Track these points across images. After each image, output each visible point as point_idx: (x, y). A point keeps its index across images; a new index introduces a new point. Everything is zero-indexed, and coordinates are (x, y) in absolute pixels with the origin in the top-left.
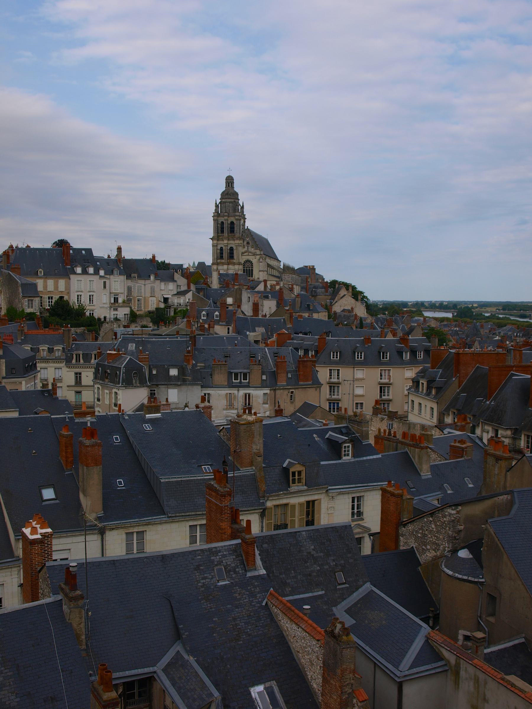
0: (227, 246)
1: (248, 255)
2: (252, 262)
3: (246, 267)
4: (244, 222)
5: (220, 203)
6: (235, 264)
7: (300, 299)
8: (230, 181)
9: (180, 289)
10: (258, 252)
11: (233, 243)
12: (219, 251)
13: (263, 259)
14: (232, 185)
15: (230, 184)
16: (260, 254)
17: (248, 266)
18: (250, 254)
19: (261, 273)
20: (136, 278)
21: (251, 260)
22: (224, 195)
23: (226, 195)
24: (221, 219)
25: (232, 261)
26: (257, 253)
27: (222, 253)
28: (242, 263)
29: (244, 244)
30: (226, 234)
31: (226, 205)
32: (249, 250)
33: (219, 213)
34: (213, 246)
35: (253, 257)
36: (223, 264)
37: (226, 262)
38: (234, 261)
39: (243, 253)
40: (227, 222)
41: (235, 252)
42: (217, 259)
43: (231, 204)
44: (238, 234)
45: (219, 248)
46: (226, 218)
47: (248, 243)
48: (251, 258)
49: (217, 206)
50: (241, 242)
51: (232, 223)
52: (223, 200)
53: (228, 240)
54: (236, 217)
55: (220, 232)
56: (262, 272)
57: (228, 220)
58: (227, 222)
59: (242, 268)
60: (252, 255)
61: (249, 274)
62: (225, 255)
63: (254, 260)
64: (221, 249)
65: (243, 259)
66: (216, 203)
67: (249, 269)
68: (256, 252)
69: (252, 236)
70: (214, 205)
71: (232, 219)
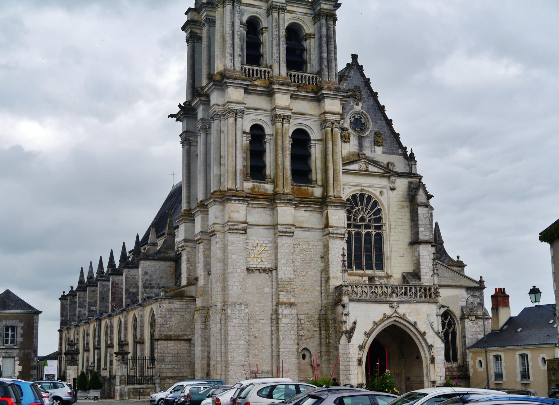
1: (366, 173)
2: (376, 203)
12: (244, 141)
17: (363, 219)
18: (372, 168)
29: (347, 125)
32: (367, 152)
35: (384, 182)
38: (318, 192)
39: (348, 161)
41: (316, 151)
45: (248, 130)
61: (368, 258)
67: (368, 235)
68: (393, 164)
69: (374, 95)
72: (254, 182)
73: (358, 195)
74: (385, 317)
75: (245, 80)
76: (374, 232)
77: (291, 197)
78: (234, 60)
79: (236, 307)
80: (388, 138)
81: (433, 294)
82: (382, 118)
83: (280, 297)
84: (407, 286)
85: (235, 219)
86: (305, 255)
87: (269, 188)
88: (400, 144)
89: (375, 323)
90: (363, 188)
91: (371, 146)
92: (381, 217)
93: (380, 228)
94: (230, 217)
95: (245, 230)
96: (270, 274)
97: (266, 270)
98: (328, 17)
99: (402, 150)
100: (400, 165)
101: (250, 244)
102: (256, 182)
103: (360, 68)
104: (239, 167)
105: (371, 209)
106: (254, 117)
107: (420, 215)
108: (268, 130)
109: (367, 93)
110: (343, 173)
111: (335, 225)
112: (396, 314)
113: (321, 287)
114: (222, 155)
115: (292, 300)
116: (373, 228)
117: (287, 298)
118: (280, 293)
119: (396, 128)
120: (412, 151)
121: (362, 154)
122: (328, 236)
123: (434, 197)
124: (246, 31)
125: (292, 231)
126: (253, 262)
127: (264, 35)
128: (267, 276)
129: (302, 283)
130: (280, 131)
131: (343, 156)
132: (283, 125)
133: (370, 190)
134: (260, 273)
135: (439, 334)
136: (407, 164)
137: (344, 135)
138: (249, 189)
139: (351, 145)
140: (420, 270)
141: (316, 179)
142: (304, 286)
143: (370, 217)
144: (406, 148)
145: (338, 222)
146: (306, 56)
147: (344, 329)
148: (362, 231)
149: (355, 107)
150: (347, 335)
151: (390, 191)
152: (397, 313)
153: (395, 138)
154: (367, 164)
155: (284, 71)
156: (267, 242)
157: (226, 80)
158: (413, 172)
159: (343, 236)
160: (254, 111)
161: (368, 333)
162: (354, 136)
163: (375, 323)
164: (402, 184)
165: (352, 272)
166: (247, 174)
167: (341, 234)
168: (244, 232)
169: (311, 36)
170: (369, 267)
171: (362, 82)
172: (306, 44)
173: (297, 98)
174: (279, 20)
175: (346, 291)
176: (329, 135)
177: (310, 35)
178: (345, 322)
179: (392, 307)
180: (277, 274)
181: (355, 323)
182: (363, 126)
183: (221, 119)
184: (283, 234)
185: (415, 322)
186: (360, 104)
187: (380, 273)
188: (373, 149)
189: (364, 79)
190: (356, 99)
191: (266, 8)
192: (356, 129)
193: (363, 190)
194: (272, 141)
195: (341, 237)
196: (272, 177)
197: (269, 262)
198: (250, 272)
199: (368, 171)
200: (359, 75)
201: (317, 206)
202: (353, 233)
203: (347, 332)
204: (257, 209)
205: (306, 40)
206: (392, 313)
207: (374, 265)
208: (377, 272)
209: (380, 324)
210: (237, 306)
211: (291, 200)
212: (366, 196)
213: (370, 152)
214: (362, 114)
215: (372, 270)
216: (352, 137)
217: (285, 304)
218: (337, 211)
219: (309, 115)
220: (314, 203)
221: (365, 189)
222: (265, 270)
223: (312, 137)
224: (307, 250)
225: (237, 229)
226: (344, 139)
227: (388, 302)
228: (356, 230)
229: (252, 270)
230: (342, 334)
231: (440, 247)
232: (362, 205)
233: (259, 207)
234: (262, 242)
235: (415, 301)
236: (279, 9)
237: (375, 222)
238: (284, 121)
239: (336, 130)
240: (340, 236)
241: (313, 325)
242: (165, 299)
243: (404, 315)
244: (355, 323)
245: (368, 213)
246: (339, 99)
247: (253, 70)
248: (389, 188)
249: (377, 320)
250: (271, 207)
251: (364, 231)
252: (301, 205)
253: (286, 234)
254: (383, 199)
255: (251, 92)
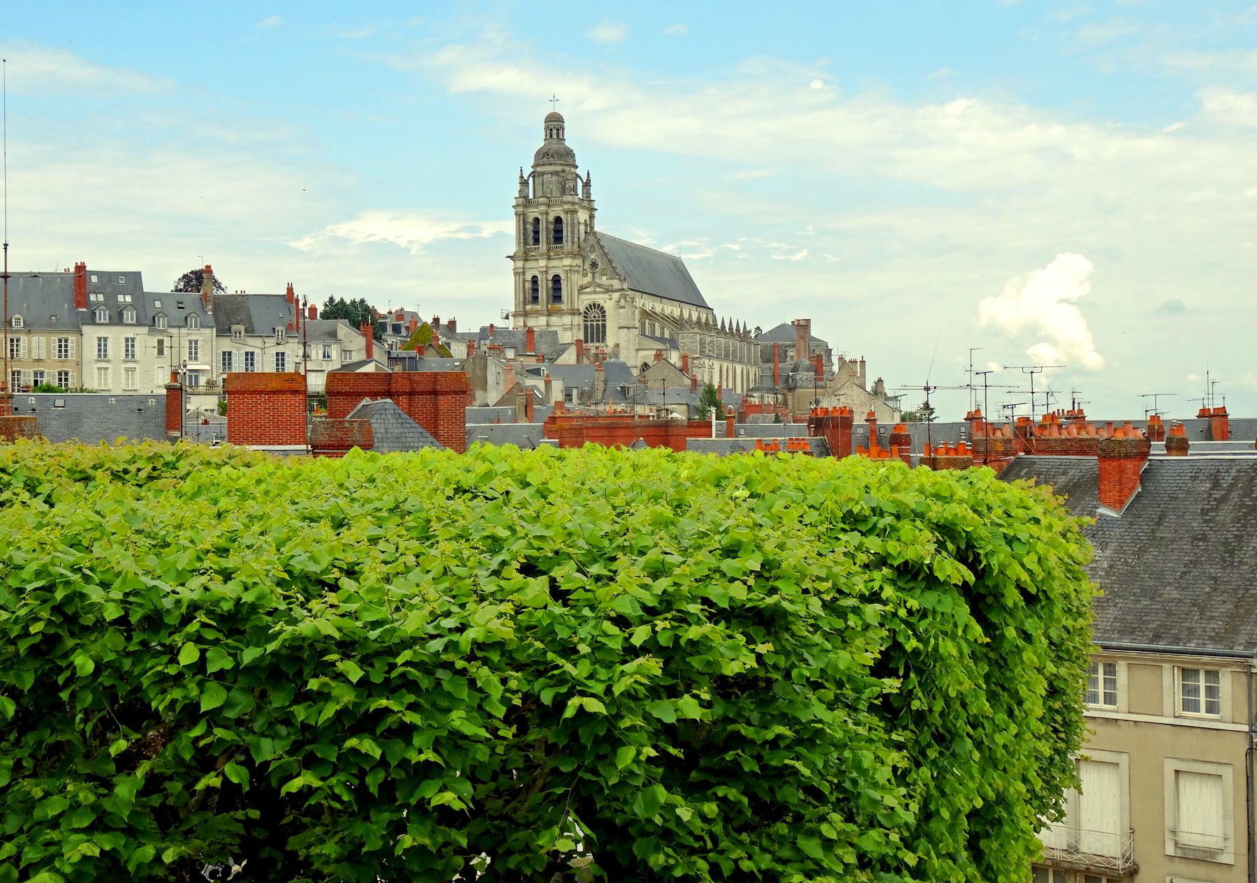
0: (546, 272)
1: (595, 292)
4: (592, 217)
5: (533, 174)
6: (564, 314)
7: (603, 373)
8: (555, 125)
9: (350, 358)
10: (616, 284)
11: (561, 265)
12: (528, 285)
13: (628, 299)
14: (558, 134)
15: (554, 132)
16: (622, 290)
18: (598, 289)
19: (623, 332)
20: (243, 333)
21: (602, 303)
22: (543, 156)
24: (533, 213)
25: (557, 306)
26: (615, 288)
27: (535, 290)
28: (582, 311)
30: (543, 246)
32: (597, 281)
33: (531, 196)
34: (516, 274)
35: (606, 296)
36: (537, 313)
37: (545, 308)
39: (582, 288)
40: (547, 219)
42: (525, 304)
43: (555, 178)
44: (570, 244)
46: (543, 208)
47: (594, 265)
48: (600, 299)
49: (524, 183)
50: (578, 262)
51: (558, 220)
52: (539, 169)
53: (549, 259)
54: (566, 207)
56: (626, 330)
57: (547, 213)
58: (547, 219)
59: (582, 323)
62: (542, 294)
63: (609, 305)
64: (535, 277)
65: (583, 302)
66: (522, 177)
69: (602, 247)
70: (518, 180)
71: (556, 211)
80: (609, 269)
108: (539, 277)
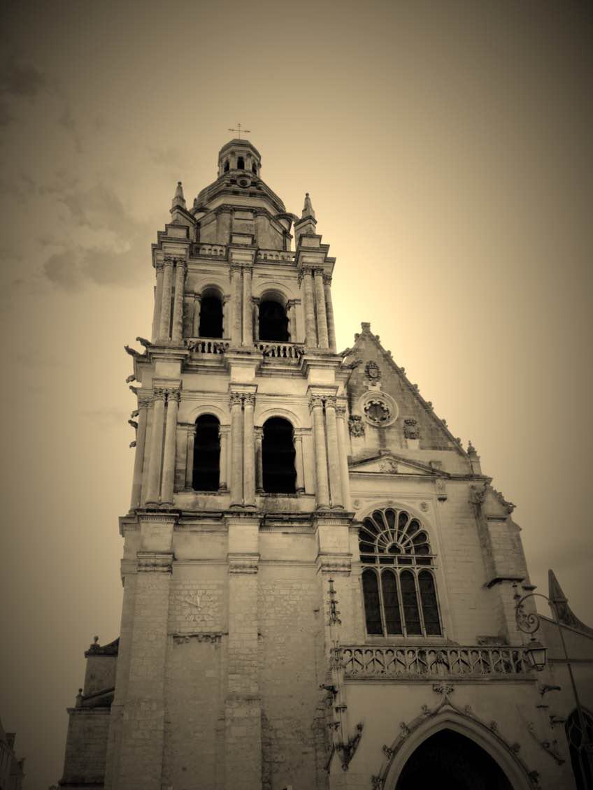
1: (394, 475)
2: (415, 523)
3: (383, 561)
12: (187, 437)
17: (394, 549)
18: (401, 469)
23: (234, 182)
24: (205, 275)
26: (447, 471)
29: (355, 413)
31: (235, 222)
32: (395, 448)
35: (426, 489)
45: (192, 420)
47: (376, 409)
55: (197, 334)
60: (422, 479)
67: (407, 575)
68: (439, 463)
69: (400, 372)
72: (197, 494)
73: (384, 512)
74: (425, 714)
75: (180, 349)
76: (418, 568)
77: (252, 510)
78: (171, 332)
79: (140, 705)
81: (523, 665)
82: (416, 401)
83: (229, 686)
84: (465, 649)
85: (150, 549)
86: (285, 607)
87: (220, 502)
88: (448, 436)
89: (404, 726)
90: (390, 500)
91: (400, 438)
92: (427, 544)
93: (428, 561)
94: (142, 546)
95: (170, 566)
96: (217, 643)
97: (210, 636)
98: (315, 273)
99: (453, 444)
100: (450, 462)
101: (183, 593)
102: (201, 494)
103: (375, 340)
104: (168, 467)
105: (409, 532)
106: (202, 403)
107: (494, 535)
108: (224, 420)
109: (389, 369)
110: (351, 477)
111: (331, 550)
112: (448, 707)
113: (316, 663)
114: (146, 455)
115: (254, 690)
116: (414, 561)
117: (243, 685)
118: (231, 676)
119: (412, 378)
120: (470, 444)
121: (384, 451)
122: (320, 572)
123: (515, 506)
124: (199, 301)
125: (255, 563)
126: (187, 623)
127: (226, 305)
128: (213, 647)
129: (279, 658)
130: (237, 415)
131: (354, 455)
132: (243, 409)
133: (404, 502)
134: (200, 641)
135: (548, 747)
136: (464, 463)
137: (355, 426)
138: (188, 505)
139: (367, 440)
140: (507, 631)
141: (304, 486)
142: (283, 663)
143: (408, 544)
144: (458, 441)
145: (337, 545)
146: (290, 328)
147: (336, 741)
148: (396, 568)
149: (370, 388)
150: (342, 753)
151: (439, 503)
152: (450, 704)
153: (440, 426)
154: (393, 464)
155: (248, 341)
156: (215, 587)
157: (150, 351)
158: (476, 472)
159: (347, 569)
160: (202, 394)
161: (390, 749)
162: (371, 426)
163: (404, 726)
164: (458, 491)
165: (381, 638)
166: (186, 483)
167: (344, 566)
168: (165, 569)
169: (294, 302)
170: (414, 629)
171: (378, 356)
172: (289, 314)
173: (271, 374)
174: (242, 282)
175: (337, 660)
176: (320, 417)
177: (294, 301)
178: (337, 725)
179: (438, 691)
180: (228, 642)
181: (360, 728)
182: (386, 413)
183: (149, 407)
184: (239, 570)
185: (493, 724)
186: (379, 384)
187: (434, 639)
188: (404, 444)
189: (381, 352)
190: (371, 377)
191: (228, 274)
192: (376, 419)
193: (391, 502)
194: (229, 434)
195: (345, 571)
196: (228, 485)
197: (218, 622)
198: (181, 640)
199: (396, 473)
200: (374, 348)
201: (304, 525)
202: (380, 571)
203: (341, 746)
204: (199, 534)
205: (290, 307)
206: (439, 704)
207: (422, 624)
208: (429, 638)
209: (416, 727)
210: (143, 704)
211: (251, 514)
212: (398, 512)
213: (399, 448)
214: (382, 398)
215: (421, 634)
216: (368, 430)
217: (238, 698)
218: (335, 528)
219: (289, 395)
220: (301, 520)
221: (396, 501)
222: (207, 636)
223: (295, 425)
224: (287, 598)
225: (155, 565)
226: (355, 432)
227: (428, 680)
228: (385, 566)
229: (184, 637)
230: (333, 751)
231: (563, 607)
232: (392, 526)
233: (203, 531)
234: (205, 587)
235: (487, 679)
236: (242, 268)
237: (416, 553)
238: (245, 402)
239: (330, 410)
240: (342, 569)
241: (303, 740)
242: (80, 710)
243: (467, 707)
244: (360, 728)
245: (404, 539)
246: (333, 368)
247: (203, 344)
248: (435, 498)
249: (409, 721)
250: (224, 529)
251: (400, 568)
252: (276, 525)
253: (244, 570)
254: (428, 515)
255: (197, 371)
